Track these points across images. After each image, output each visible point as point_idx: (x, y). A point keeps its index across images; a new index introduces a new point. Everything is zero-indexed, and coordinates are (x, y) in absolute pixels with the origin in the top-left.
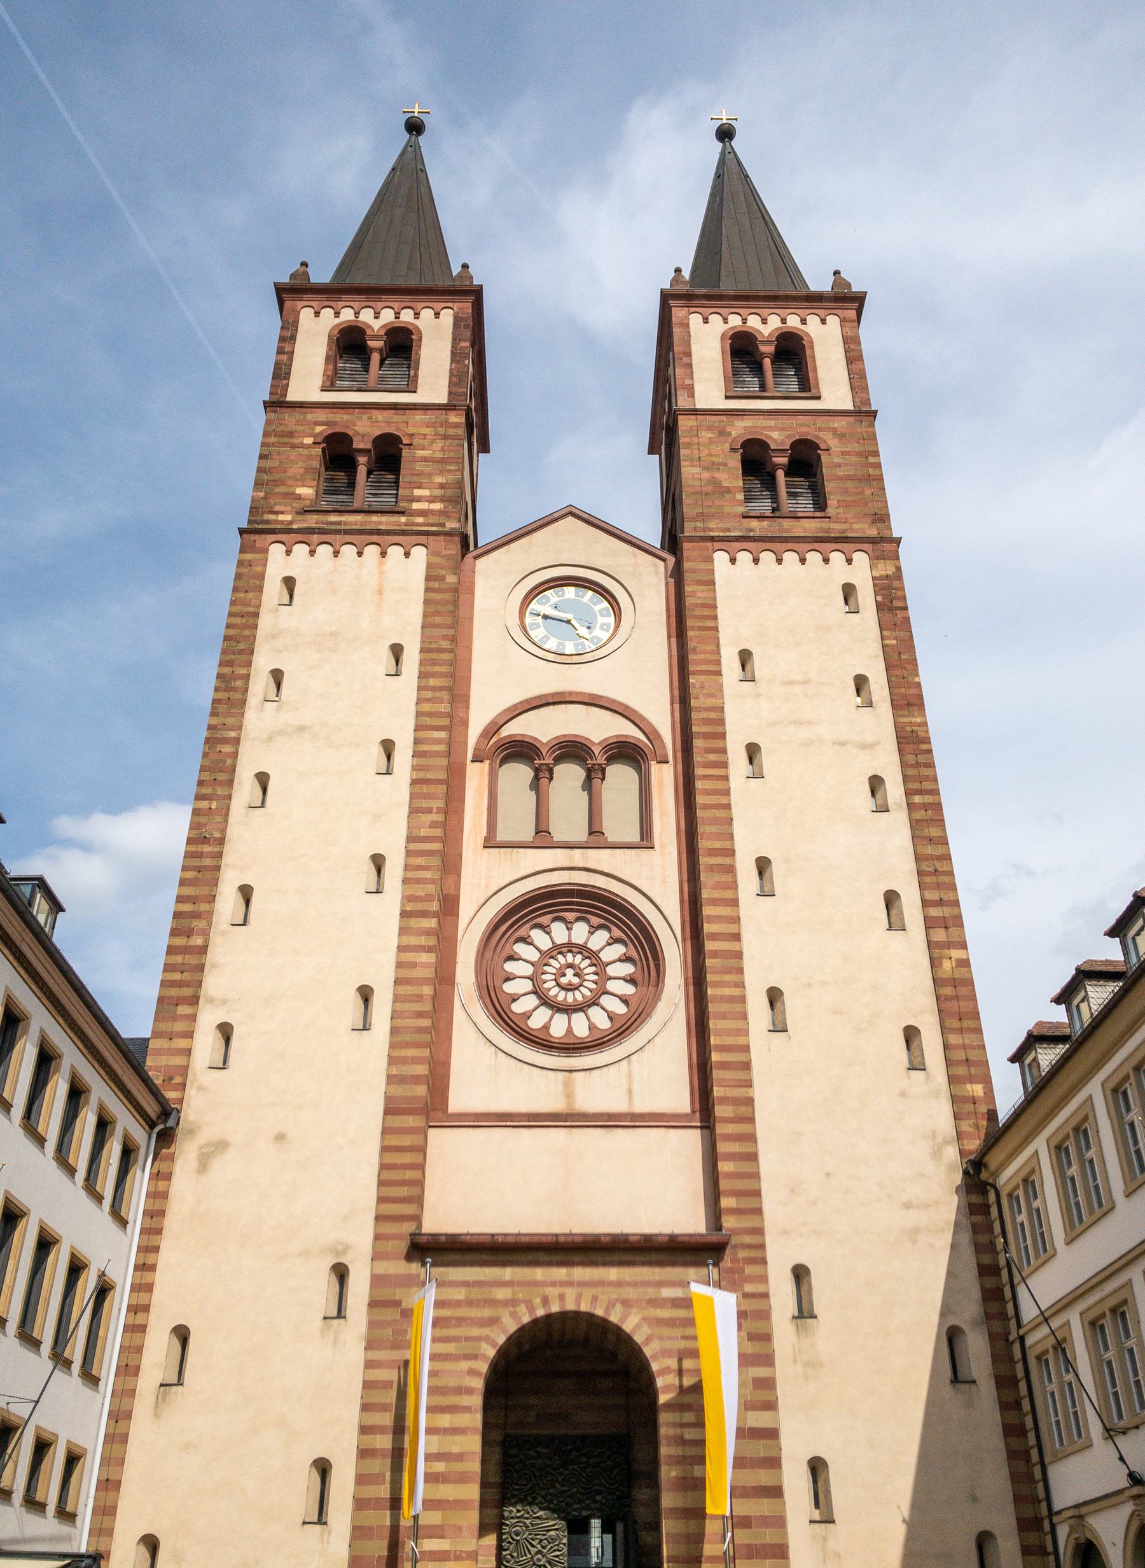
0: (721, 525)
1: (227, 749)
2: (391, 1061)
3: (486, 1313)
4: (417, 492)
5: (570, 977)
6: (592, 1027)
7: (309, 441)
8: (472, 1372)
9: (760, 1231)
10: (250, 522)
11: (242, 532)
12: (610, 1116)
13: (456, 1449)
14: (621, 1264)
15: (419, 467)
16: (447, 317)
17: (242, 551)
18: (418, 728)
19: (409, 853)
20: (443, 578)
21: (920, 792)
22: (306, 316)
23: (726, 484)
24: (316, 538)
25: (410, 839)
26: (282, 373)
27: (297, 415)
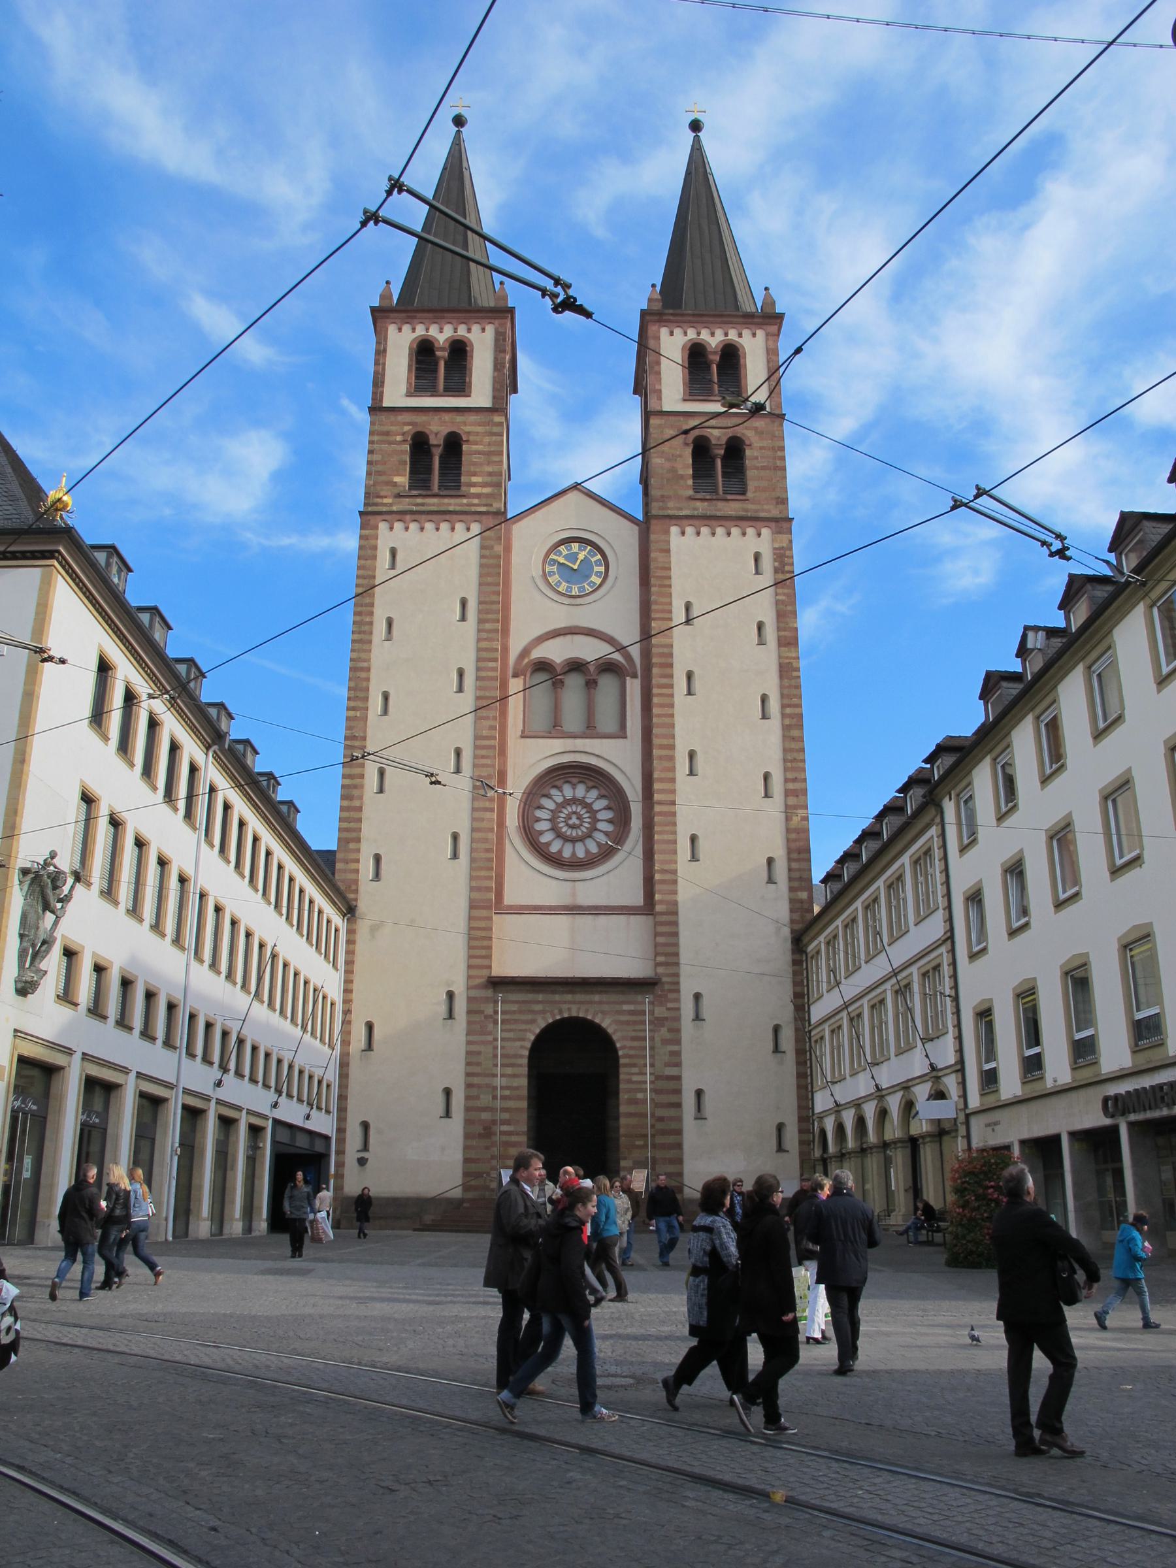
0: (677, 505)
1: (363, 675)
2: (472, 878)
3: (530, 1017)
4: (474, 479)
5: (574, 820)
6: (587, 851)
7: (399, 438)
8: (522, 1047)
9: (677, 975)
10: (366, 505)
11: (361, 513)
12: (596, 908)
13: (515, 1084)
14: (601, 992)
15: (475, 459)
16: (490, 330)
17: (362, 528)
18: (479, 660)
19: (476, 747)
20: (492, 548)
21: (789, 706)
22: (392, 329)
23: (681, 472)
24: (408, 517)
25: (477, 737)
26: (378, 382)
27: (392, 417)
